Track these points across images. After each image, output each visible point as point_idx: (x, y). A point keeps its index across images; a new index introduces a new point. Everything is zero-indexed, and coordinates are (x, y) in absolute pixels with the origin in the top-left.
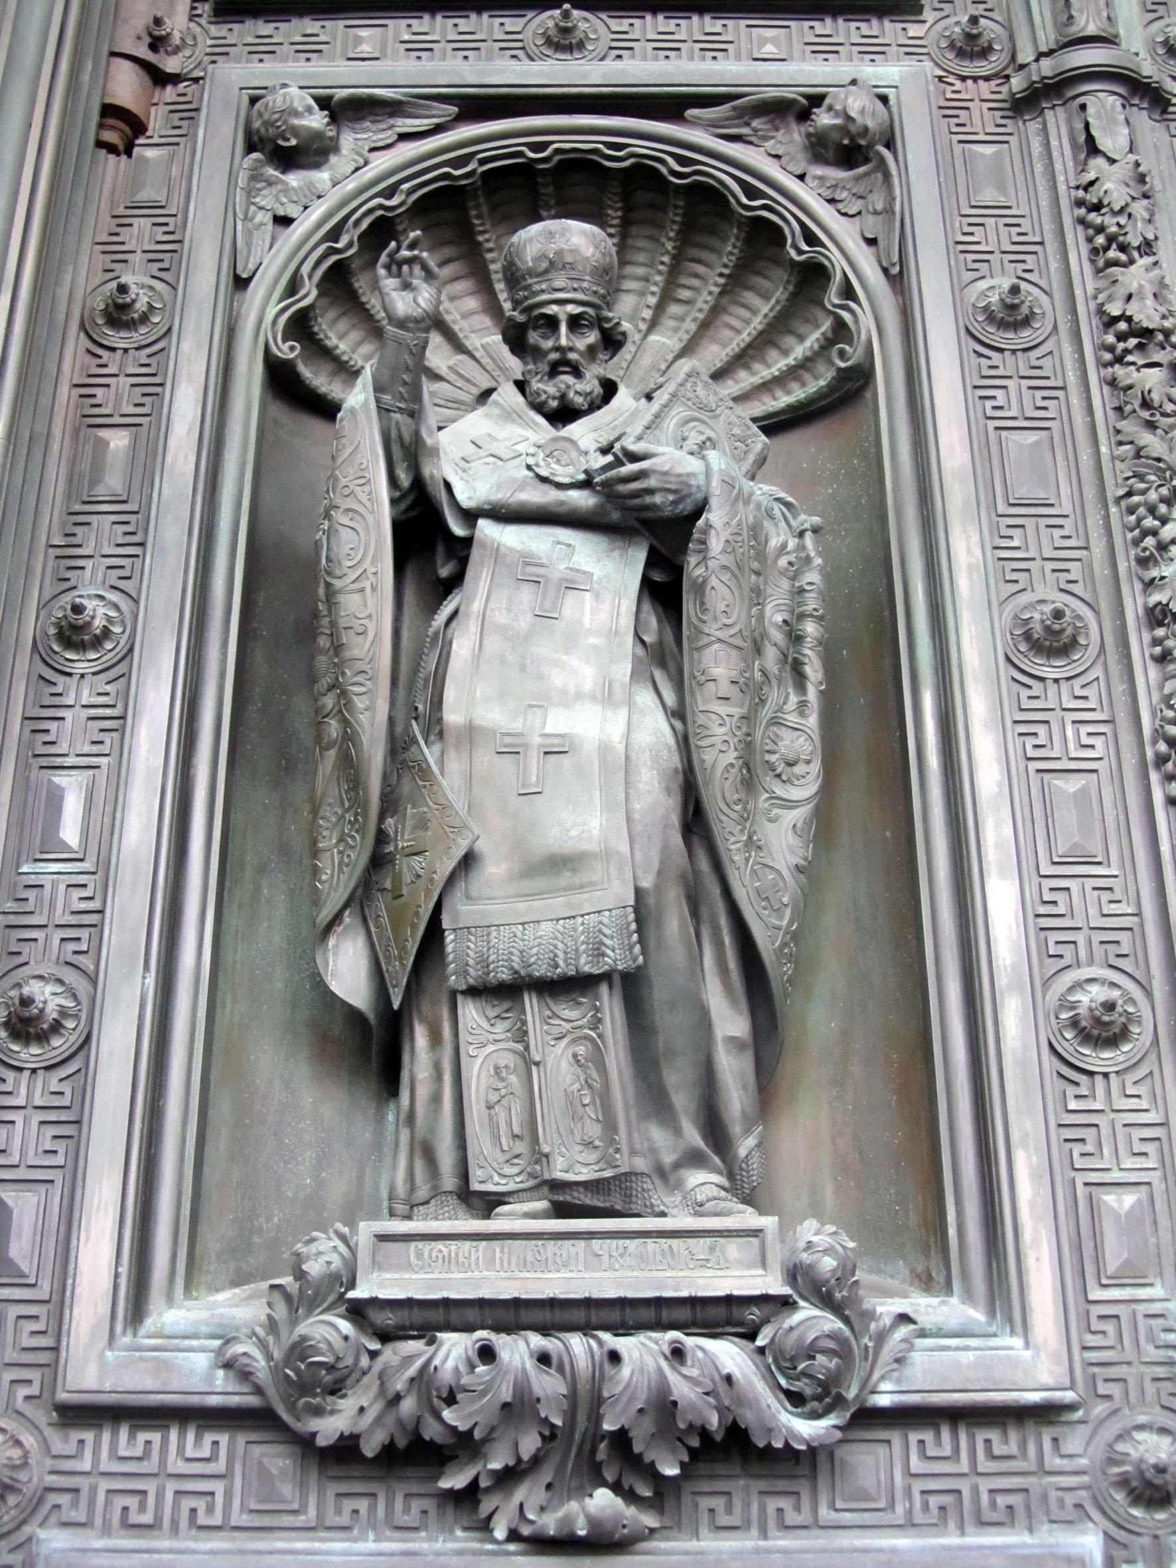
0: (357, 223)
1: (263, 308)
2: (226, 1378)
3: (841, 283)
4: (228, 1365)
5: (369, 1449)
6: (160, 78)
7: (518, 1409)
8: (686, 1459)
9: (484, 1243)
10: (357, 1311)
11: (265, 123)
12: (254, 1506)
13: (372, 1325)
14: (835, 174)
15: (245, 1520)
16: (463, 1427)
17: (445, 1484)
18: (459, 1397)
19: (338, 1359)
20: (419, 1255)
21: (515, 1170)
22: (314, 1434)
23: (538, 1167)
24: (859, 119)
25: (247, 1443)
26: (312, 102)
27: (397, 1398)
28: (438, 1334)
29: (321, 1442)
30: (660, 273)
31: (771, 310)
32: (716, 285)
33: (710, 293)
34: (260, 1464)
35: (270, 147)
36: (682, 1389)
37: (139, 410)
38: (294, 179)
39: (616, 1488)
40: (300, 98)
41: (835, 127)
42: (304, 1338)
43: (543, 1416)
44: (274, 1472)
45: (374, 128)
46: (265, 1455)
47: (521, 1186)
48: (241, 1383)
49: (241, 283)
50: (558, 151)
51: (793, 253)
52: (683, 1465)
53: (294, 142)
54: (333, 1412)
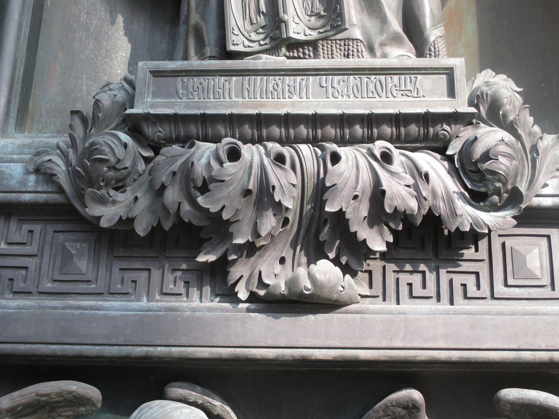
2: (37, 182)
4: (37, 171)
5: (141, 229)
8: (391, 239)
9: (234, 78)
10: (135, 126)
12: (58, 277)
13: (146, 138)
15: (49, 286)
16: (214, 209)
17: (202, 258)
18: (211, 186)
19: (119, 160)
20: (185, 88)
21: (262, 36)
22: (99, 218)
23: (278, 32)
25: (55, 232)
27: (163, 187)
28: (196, 141)
29: (104, 224)
34: (64, 247)
39: (336, 261)
42: (93, 144)
43: (277, 200)
44: (73, 252)
46: (67, 240)
47: (265, 47)
48: (47, 185)
52: (388, 244)
54: (114, 202)
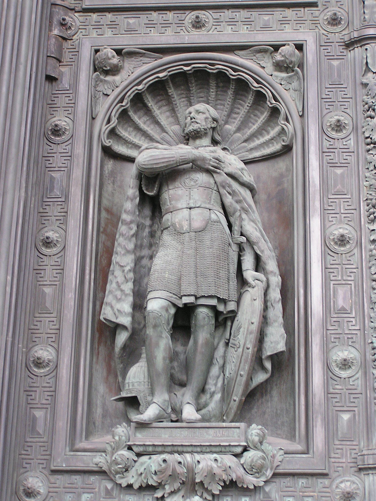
0: (129, 96)
1: (101, 127)
3: (284, 114)
6: (64, 39)
7: (173, 476)
11: (99, 62)
14: (284, 75)
24: (290, 58)
26: (115, 53)
30: (228, 104)
31: (263, 119)
32: (246, 109)
33: (244, 112)
35: (101, 70)
36: (217, 471)
37: (64, 165)
38: (109, 78)
40: (110, 53)
41: (282, 61)
45: (135, 60)
49: (93, 119)
50: (194, 68)
51: (269, 103)
53: (108, 68)
